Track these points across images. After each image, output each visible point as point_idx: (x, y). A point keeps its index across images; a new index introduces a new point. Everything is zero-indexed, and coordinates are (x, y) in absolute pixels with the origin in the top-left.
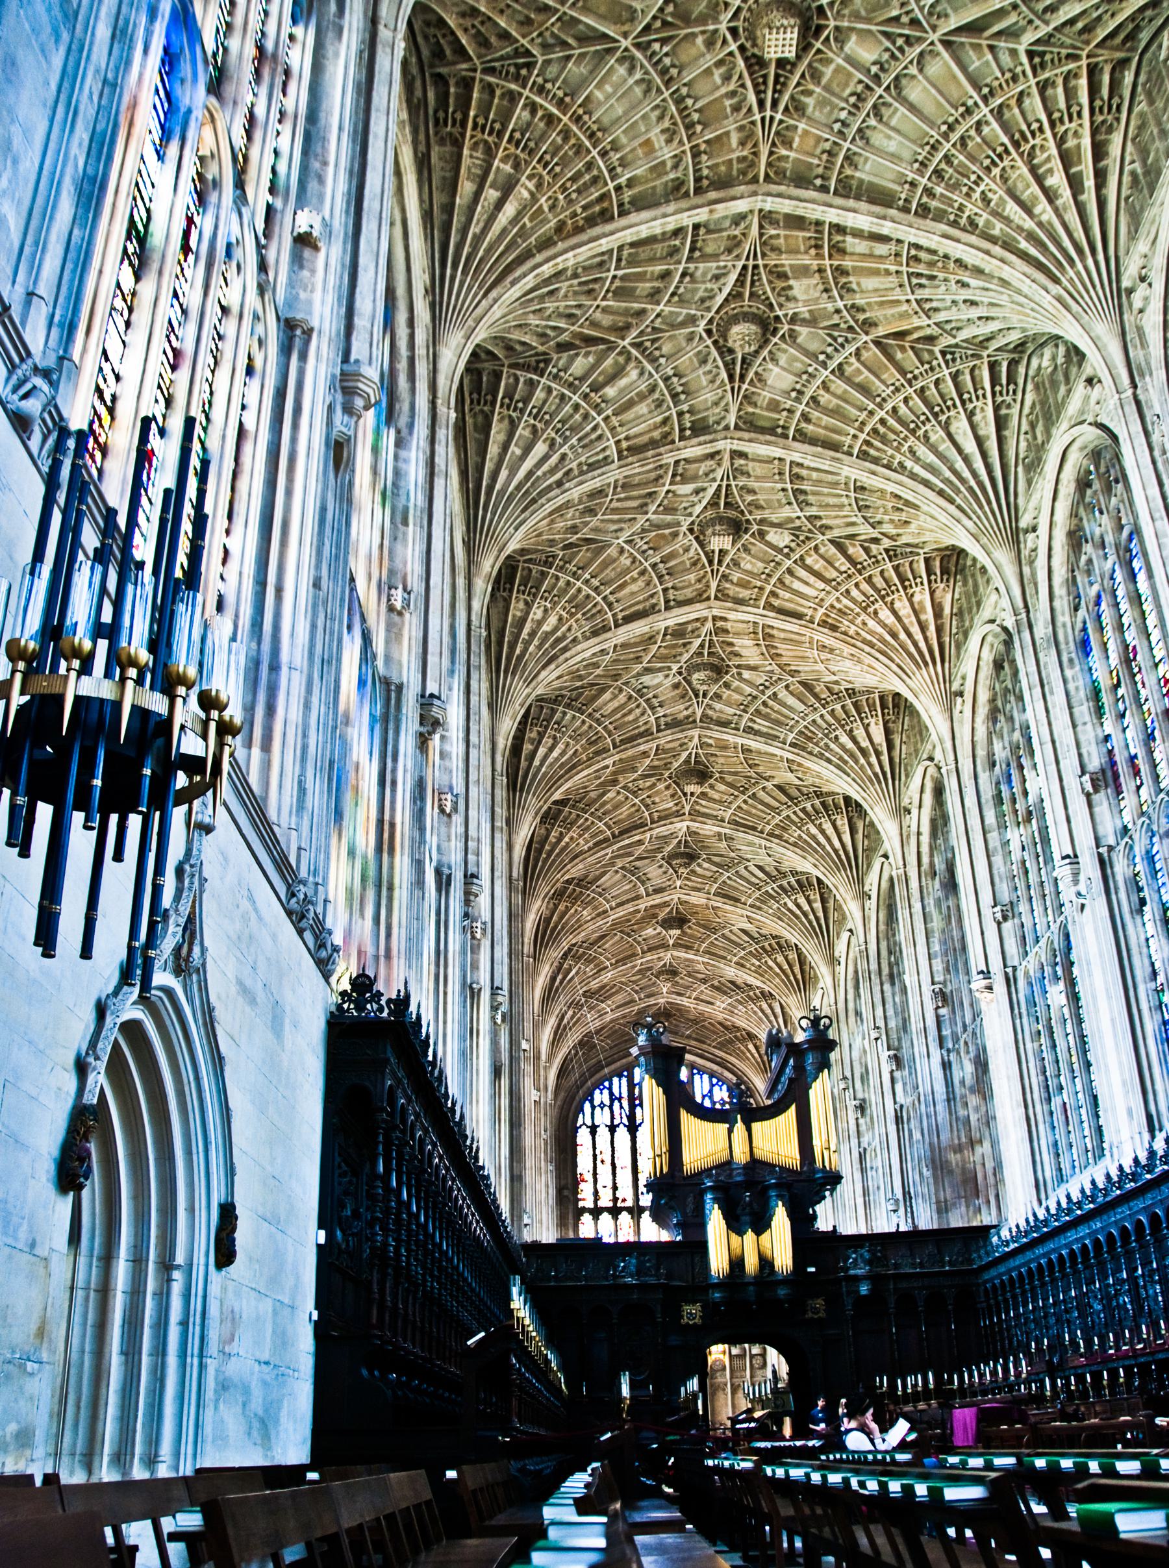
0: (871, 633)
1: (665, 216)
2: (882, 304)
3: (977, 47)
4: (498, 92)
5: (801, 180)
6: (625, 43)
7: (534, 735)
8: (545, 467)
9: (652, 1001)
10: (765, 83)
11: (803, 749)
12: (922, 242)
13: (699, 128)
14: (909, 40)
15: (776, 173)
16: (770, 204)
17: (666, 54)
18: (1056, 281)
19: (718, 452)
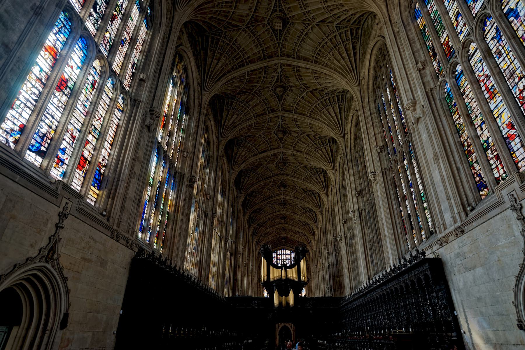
0: (317, 156)
1: (257, 65)
2: (310, 83)
3: (324, 25)
4: (215, 38)
5: (288, 56)
6: (243, 27)
7: (244, 178)
8: (237, 120)
9: (280, 235)
10: (277, 34)
11: (306, 181)
12: (316, 69)
13: (263, 45)
14: (309, 24)
15: (283, 54)
16: (281, 61)
17: (254, 29)
18: (346, 78)
19: (278, 116)
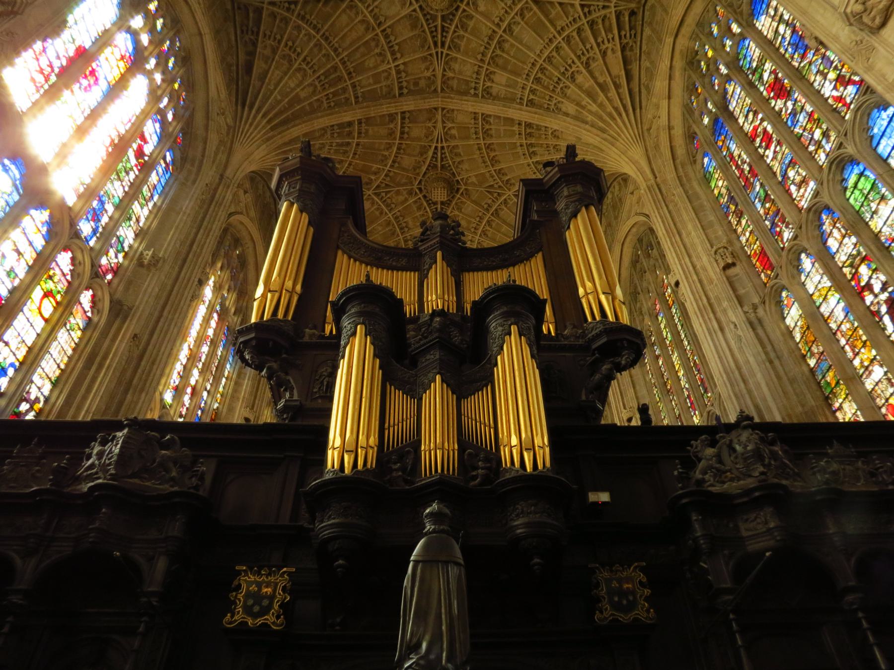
7: (268, 52)
11: (540, 107)
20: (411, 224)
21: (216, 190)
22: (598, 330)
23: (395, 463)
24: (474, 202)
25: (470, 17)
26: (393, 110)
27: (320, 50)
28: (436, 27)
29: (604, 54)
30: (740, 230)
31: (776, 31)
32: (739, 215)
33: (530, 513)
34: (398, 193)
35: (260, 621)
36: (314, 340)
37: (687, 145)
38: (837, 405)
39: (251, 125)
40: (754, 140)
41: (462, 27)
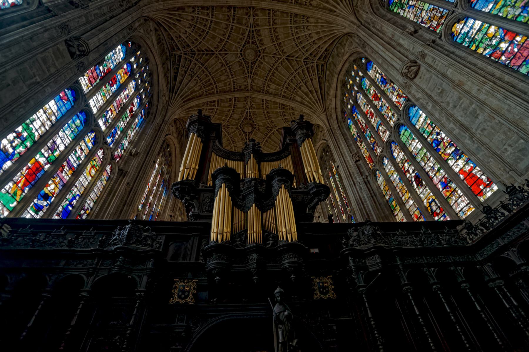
7: (183, 72)
11: (288, 98)
20: (236, 141)
21: (161, 125)
22: (313, 186)
23: (238, 238)
24: (261, 133)
25: (262, 63)
26: (231, 97)
27: (204, 73)
28: (249, 66)
29: (312, 80)
30: (361, 148)
31: (376, 76)
32: (361, 142)
33: (291, 258)
34: (232, 128)
35: (184, 301)
36: (203, 188)
37: (342, 115)
38: (396, 214)
39: (175, 100)
40: (367, 115)
41: (259, 67)
